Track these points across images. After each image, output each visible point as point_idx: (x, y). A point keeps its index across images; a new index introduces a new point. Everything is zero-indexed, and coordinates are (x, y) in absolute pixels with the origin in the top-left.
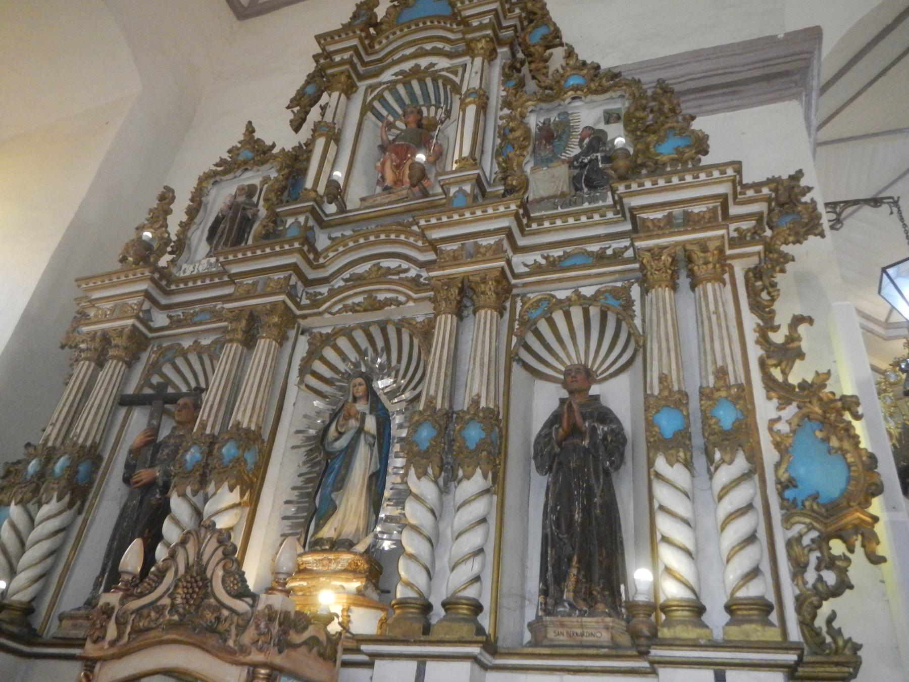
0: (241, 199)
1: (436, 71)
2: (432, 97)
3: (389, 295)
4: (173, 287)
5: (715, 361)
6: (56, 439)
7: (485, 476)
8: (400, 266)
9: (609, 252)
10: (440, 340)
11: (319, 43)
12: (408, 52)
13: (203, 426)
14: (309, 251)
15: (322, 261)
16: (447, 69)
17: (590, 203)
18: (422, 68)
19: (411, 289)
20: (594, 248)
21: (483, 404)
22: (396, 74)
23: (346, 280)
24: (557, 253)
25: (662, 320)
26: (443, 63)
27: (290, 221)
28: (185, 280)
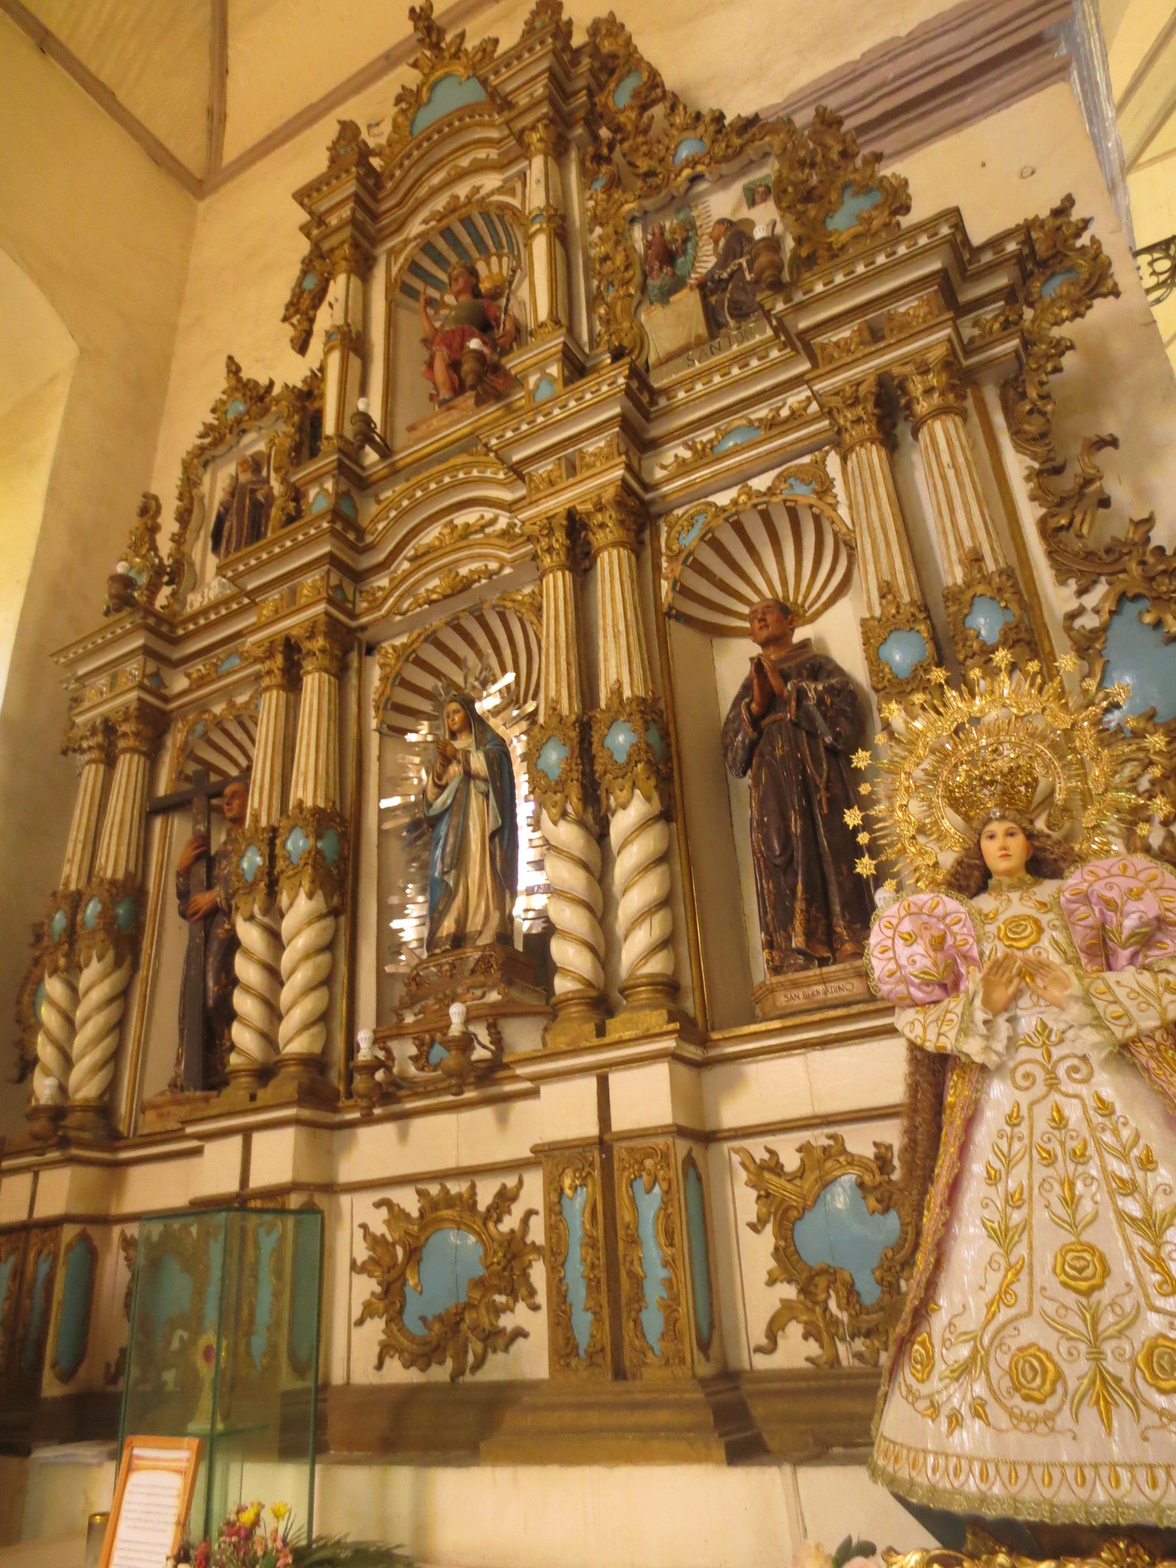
0: (244, 478)
1: (483, 199)
2: (490, 243)
3: (474, 566)
4: (181, 632)
5: (959, 543)
6: (78, 879)
7: (648, 799)
8: (482, 517)
9: (785, 413)
10: (552, 613)
11: (302, 204)
12: (437, 179)
13: (256, 818)
14: (345, 529)
15: (369, 539)
16: (499, 190)
17: (740, 342)
18: (462, 199)
19: (502, 548)
20: (762, 412)
21: (627, 693)
22: (425, 222)
23: (411, 560)
24: (706, 435)
25: (872, 499)
26: (490, 182)
27: (313, 493)
28: (193, 618)
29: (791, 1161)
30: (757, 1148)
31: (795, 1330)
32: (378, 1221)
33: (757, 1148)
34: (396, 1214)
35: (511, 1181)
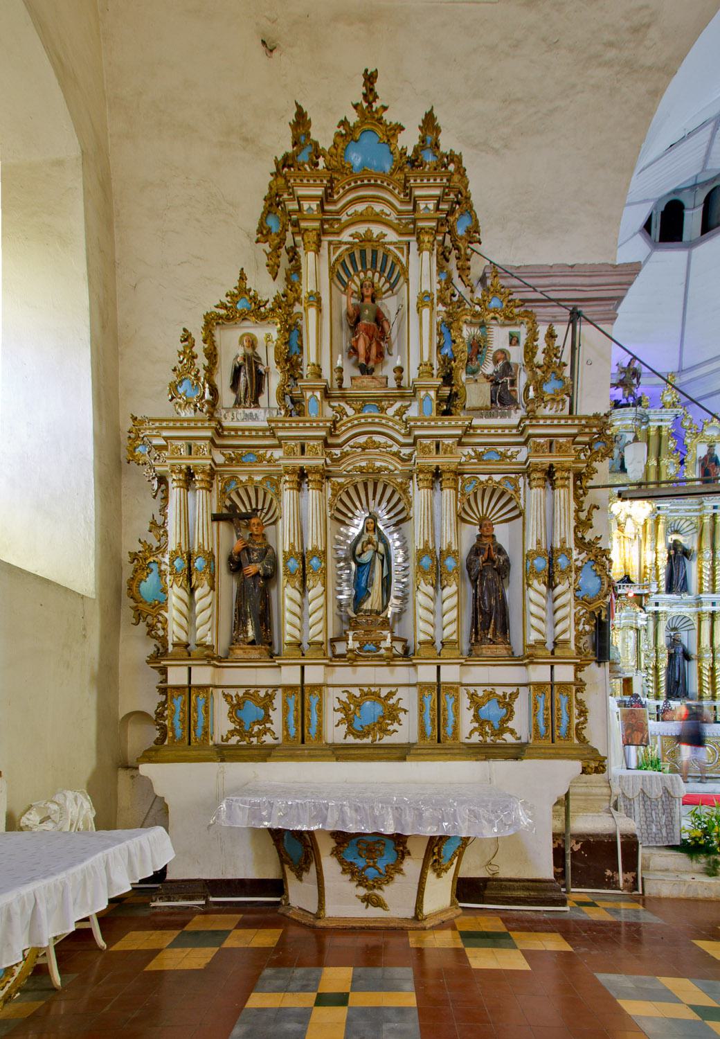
1: (386, 243)
2: (379, 265)
4: (226, 433)
15: (337, 433)
18: (375, 236)
24: (481, 449)
29: (480, 694)
30: (472, 690)
31: (477, 733)
32: (344, 697)
33: (472, 690)
34: (351, 696)
35: (394, 689)
